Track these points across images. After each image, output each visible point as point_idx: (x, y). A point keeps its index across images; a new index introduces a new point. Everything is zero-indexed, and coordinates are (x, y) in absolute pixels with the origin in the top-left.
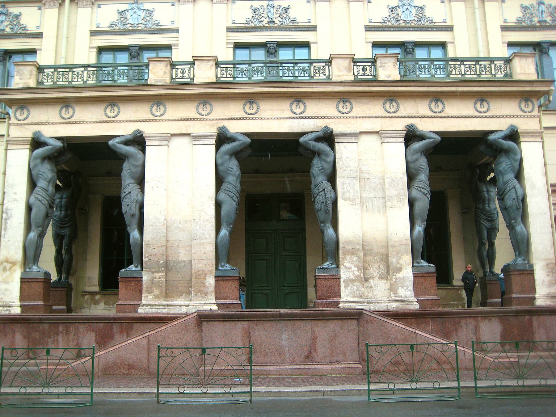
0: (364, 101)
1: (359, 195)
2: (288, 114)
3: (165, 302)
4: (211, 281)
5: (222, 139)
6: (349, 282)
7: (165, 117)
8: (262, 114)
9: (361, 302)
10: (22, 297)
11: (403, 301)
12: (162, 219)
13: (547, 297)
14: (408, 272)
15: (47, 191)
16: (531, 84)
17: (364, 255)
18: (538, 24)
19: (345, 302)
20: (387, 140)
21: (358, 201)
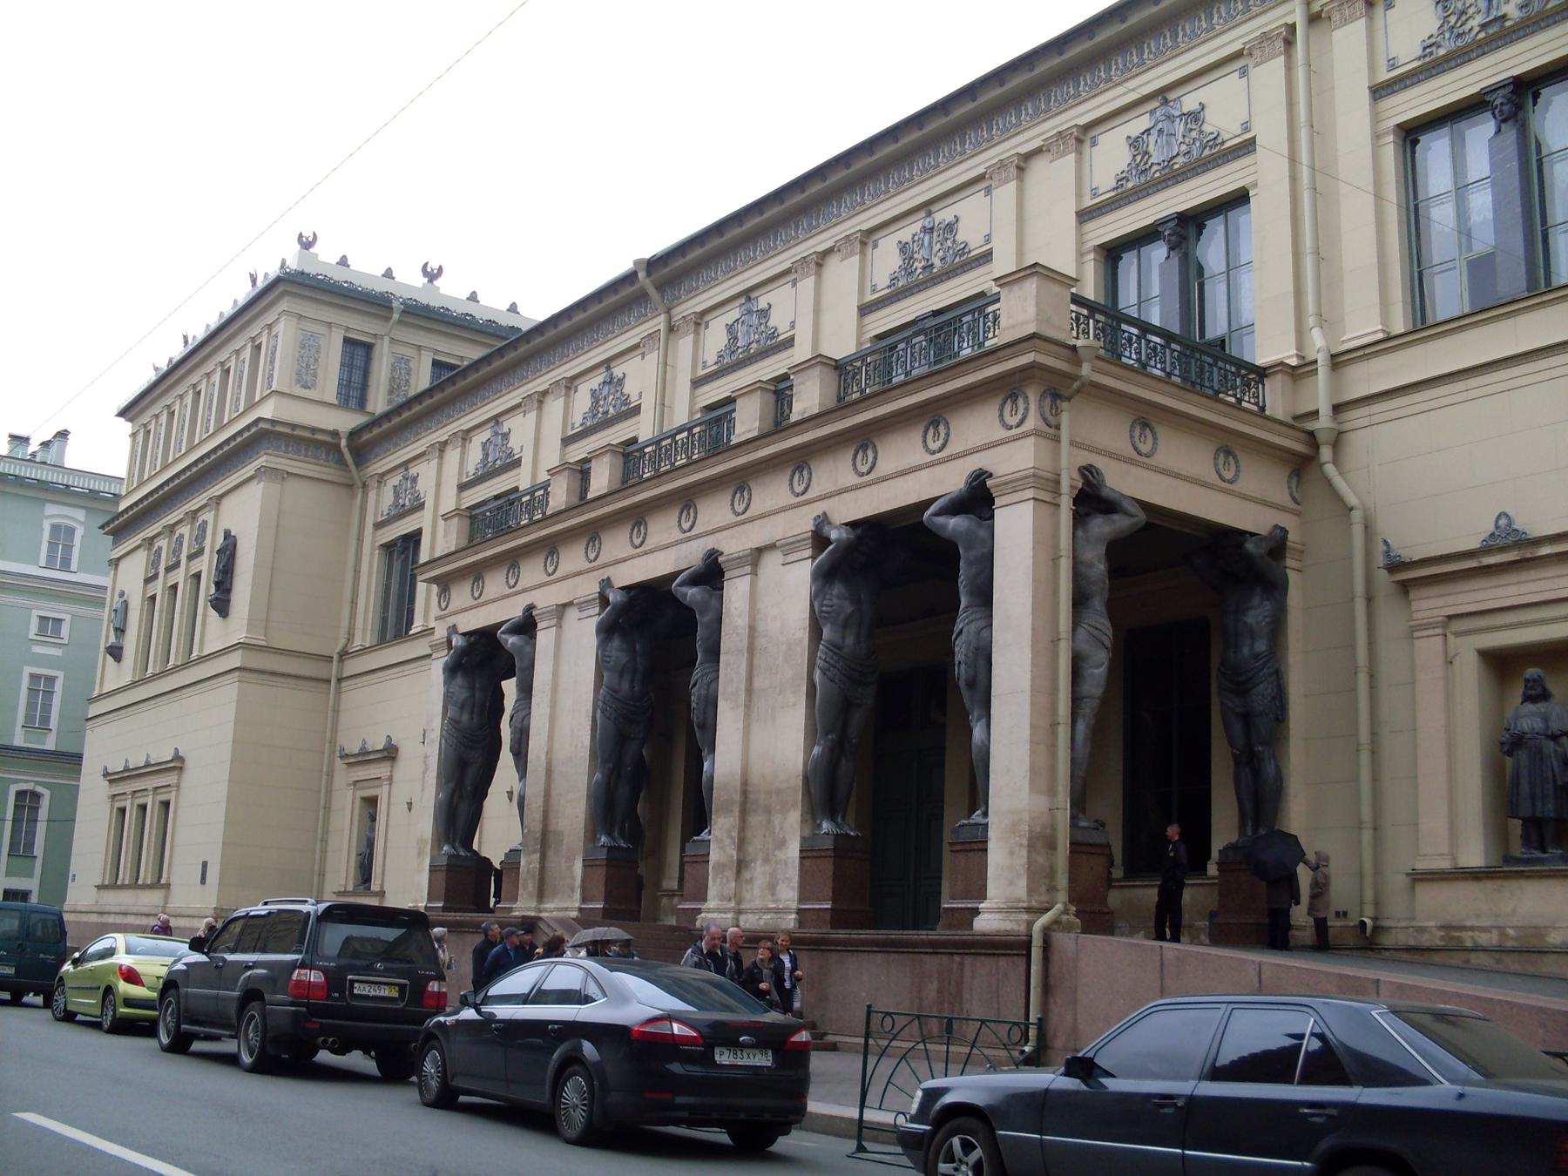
1: (743, 686)
5: (603, 600)
6: (721, 867)
8: (651, 543)
9: (725, 911)
11: (777, 911)
12: (543, 757)
13: (999, 910)
14: (793, 850)
15: (458, 722)
16: (994, 356)
17: (744, 813)
19: (709, 911)
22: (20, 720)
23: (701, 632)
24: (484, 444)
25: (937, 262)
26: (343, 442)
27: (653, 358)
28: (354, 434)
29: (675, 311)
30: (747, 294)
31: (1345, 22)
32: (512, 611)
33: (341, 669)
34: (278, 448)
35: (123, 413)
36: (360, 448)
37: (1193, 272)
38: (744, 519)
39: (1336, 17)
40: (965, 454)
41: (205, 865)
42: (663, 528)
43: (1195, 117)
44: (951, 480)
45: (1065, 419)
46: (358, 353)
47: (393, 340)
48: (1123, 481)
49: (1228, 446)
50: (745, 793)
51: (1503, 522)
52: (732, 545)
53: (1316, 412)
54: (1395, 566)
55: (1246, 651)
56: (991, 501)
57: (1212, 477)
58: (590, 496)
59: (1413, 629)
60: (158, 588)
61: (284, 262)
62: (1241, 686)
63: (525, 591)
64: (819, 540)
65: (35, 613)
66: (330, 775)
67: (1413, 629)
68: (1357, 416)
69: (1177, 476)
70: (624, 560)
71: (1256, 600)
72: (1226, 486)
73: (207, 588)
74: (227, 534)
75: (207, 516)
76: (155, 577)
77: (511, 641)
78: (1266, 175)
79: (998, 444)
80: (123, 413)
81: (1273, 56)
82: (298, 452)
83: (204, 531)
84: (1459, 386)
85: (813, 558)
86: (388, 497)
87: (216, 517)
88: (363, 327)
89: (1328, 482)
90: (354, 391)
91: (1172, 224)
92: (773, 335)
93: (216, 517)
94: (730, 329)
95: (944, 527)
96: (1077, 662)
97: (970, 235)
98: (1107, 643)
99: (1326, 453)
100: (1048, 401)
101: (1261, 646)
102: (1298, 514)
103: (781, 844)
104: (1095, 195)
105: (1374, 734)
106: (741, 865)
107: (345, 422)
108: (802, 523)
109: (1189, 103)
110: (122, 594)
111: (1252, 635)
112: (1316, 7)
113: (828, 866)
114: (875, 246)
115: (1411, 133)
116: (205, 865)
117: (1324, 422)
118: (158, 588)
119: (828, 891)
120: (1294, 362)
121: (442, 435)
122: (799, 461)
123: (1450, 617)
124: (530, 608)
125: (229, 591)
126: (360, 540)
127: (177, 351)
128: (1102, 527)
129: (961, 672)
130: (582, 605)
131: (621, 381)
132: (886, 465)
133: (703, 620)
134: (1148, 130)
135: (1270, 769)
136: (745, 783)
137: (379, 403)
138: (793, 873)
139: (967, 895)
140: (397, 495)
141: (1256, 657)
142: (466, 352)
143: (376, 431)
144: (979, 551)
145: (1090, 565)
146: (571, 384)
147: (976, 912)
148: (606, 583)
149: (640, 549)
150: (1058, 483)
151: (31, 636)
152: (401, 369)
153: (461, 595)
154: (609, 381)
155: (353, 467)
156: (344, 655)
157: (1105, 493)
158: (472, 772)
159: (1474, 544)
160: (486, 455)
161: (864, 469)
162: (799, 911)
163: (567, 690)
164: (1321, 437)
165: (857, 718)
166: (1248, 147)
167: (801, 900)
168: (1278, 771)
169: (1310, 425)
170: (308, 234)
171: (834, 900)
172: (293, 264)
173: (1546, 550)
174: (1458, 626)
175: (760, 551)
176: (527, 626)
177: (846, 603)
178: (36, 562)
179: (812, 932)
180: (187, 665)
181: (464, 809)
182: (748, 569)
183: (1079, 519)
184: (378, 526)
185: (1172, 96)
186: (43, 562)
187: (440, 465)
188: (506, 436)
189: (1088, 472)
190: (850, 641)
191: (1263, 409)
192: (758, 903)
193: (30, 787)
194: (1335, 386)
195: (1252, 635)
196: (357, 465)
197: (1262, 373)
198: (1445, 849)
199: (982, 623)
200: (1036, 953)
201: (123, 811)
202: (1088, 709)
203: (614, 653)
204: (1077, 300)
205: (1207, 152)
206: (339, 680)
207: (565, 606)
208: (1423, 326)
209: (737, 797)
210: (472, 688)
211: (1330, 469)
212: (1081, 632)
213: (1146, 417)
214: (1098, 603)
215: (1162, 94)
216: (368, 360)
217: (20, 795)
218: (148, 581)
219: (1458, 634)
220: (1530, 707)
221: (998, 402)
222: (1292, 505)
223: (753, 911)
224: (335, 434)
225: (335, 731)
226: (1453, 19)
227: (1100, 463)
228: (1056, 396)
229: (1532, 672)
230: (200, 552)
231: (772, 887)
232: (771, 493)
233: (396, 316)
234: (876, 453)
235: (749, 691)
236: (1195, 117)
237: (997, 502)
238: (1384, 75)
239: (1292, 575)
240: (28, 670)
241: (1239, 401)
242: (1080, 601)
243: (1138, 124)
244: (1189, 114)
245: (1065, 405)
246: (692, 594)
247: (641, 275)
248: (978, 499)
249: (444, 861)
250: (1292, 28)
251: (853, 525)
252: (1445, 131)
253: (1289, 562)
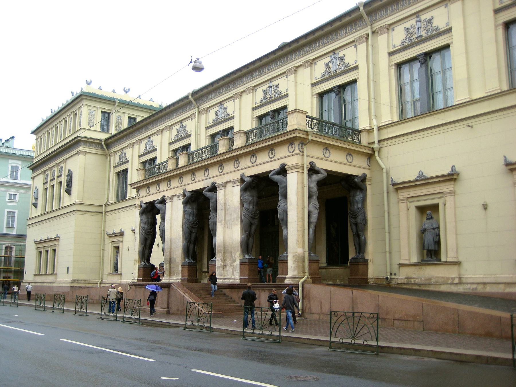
0: (228, 163)
2: (204, 178)
3: (168, 278)
4: (180, 268)
5: (184, 195)
7: (171, 187)
8: (196, 180)
10: (138, 277)
11: (234, 279)
14: (238, 263)
17: (225, 253)
18: (416, 40)
20: (234, 185)
21: (223, 222)
22: (5, 225)
23: (211, 204)
24: (146, 144)
25: (273, 97)
26: (103, 143)
27: (194, 121)
28: (106, 140)
29: (200, 107)
30: (220, 103)
31: (381, 34)
32: (159, 197)
33: (105, 209)
34: (84, 145)
35: (33, 133)
37: (342, 101)
38: (222, 174)
39: (379, 32)
40: (279, 159)
41: (68, 268)
42: (200, 175)
43: (342, 58)
44: (275, 166)
45: (305, 150)
46: (106, 116)
48: (320, 165)
49: (350, 153)
50: (225, 247)
51: (420, 173)
52: (219, 181)
53: (374, 142)
54: (394, 184)
55: (356, 207)
56: (286, 171)
57: (346, 162)
58: (179, 166)
59: (399, 201)
60: (48, 186)
61: (82, 89)
62: (355, 217)
63: (162, 192)
64: (242, 180)
66: (104, 240)
67: (399, 201)
68: (384, 143)
69: (336, 162)
70: (190, 184)
71: (358, 193)
72: (349, 164)
73: (64, 186)
74: (69, 171)
75: (63, 165)
76: (47, 182)
77: (159, 206)
78: (361, 75)
80: (33, 133)
81: (363, 43)
82: (89, 146)
83: (62, 169)
84: (411, 136)
85: (241, 185)
86: (117, 159)
87: (65, 165)
88: (107, 108)
89: (377, 161)
90: (106, 126)
91: (336, 88)
92: (228, 115)
93: (65, 165)
94: (216, 113)
95: (274, 179)
96: (310, 213)
97: (282, 89)
98: (317, 208)
99: (376, 154)
100: (300, 145)
101: (360, 205)
102: (370, 169)
103: (235, 261)
104: (316, 79)
105: (389, 228)
106: (224, 266)
107: (103, 136)
108: (237, 176)
109: (341, 54)
110: (36, 188)
111: (357, 203)
112: (374, 30)
113: (247, 267)
114: (256, 91)
115: (399, 66)
116: (68, 268)
117: (376, 145)
118: (48, 186)
119: (247, 273)
120: (368, 128)
121: (133, 141)
122: (236, 159)
123: (408, 198)
124: (164, 197)
125: (71, 187)
126: (109, 171)
127: (49, 114)
128: (315, 178)
129: (280, 216)
130: (178, 196)
131: (185, 127)
132: (259, 161)
133: (212, 201)
134: (330, 61)
135: (363, 238)
136: (225, 245)
137: (113, 131)
138: (238, 268)
139: (282, 274)
140: (120, 158)
141: (358, 208)
143: (113, 139)
144: (283, 185)
145: (313, 188)
146: (171, 127)
147: (285, 278)
148: (184, 191)
149: (194, 181)
150: (303, 167)
151: (7, 200)
153: (143, 192)
154: (182, 127)
155: (106, 150)
156: (106, 205)
157: (316, 169)
158: (148, 242)
159: (413, 178)
160: (146, 147)
161: (253, 162)
162: (240, 279)
163: (174, 221)
164: (375, 149)
165: (253, 227)
166: (356, 68)
167: (240, 276)
168: (365, 238)
169: (372, 146)
170: (89, 80)
171: (249, 276)
172: (85, 90)
173: (432, 181)
174: (410, 200)
175: (226, 182)
176: (163, 201)
177: (250, 197)
179: (244, 284)
180: (59, 209)
181: (147, 252)
182: (223, 188)
183: (309, 176)
184: (115, 167)
185: (336, 52)
187: (133, 149)
188: (152, 142)
189: (311, 163)
190: (251, 207)
191: (360, 141)
192: (229, 277)
194: (379, 135)
195: (357, 203)
196: (108, 149)
197: (360, 132)
198: (407, 258)
199: (285, 204)
200: (300, 289)
201: (41, 252)
202: (312, 226)
203: (188, 210)
204: (308, 117)
205: (346, 68)
206: (105, 212)
207: (173, 196)
208: (403, 119)
209: (223, 249)
210: (148, 218)
211: (378, 158)
212: (311, 205)
213: (327, 147)
214: (315, 198)
215: (334, 51)
216: (109, 118)
217: (6, 248)
218: (44, 184)
219: (410, 202)
220: (428, 221)
221: (287, 145)
222: (368, 167)
223: (228, 279)
224: (100, 140)
225: (105, 227)
226: (409, 35)
227: (315, 161)
228: (302, 144)
229: (428, 212)
230: (61, 175)
231: (233, 273)
232: (229, 167)
233: (117, 104)
234: (256, 157)
235: (225, 220)
236: (342, 58)
237: (288, 172)
238: (392, 50)
239: (368, 187)
240: (6, 210)
241: (353, 140)
242: (310, 197)
243: (327, 60)
244: (341, 57)
245: (305, 146)
246: (209, 194)
247: (190, 97)
248: (283, 171)
249: (142, 266)
250: (368, 35)
251: (251, 176)
252: (408, 64)
253: (367, 183)
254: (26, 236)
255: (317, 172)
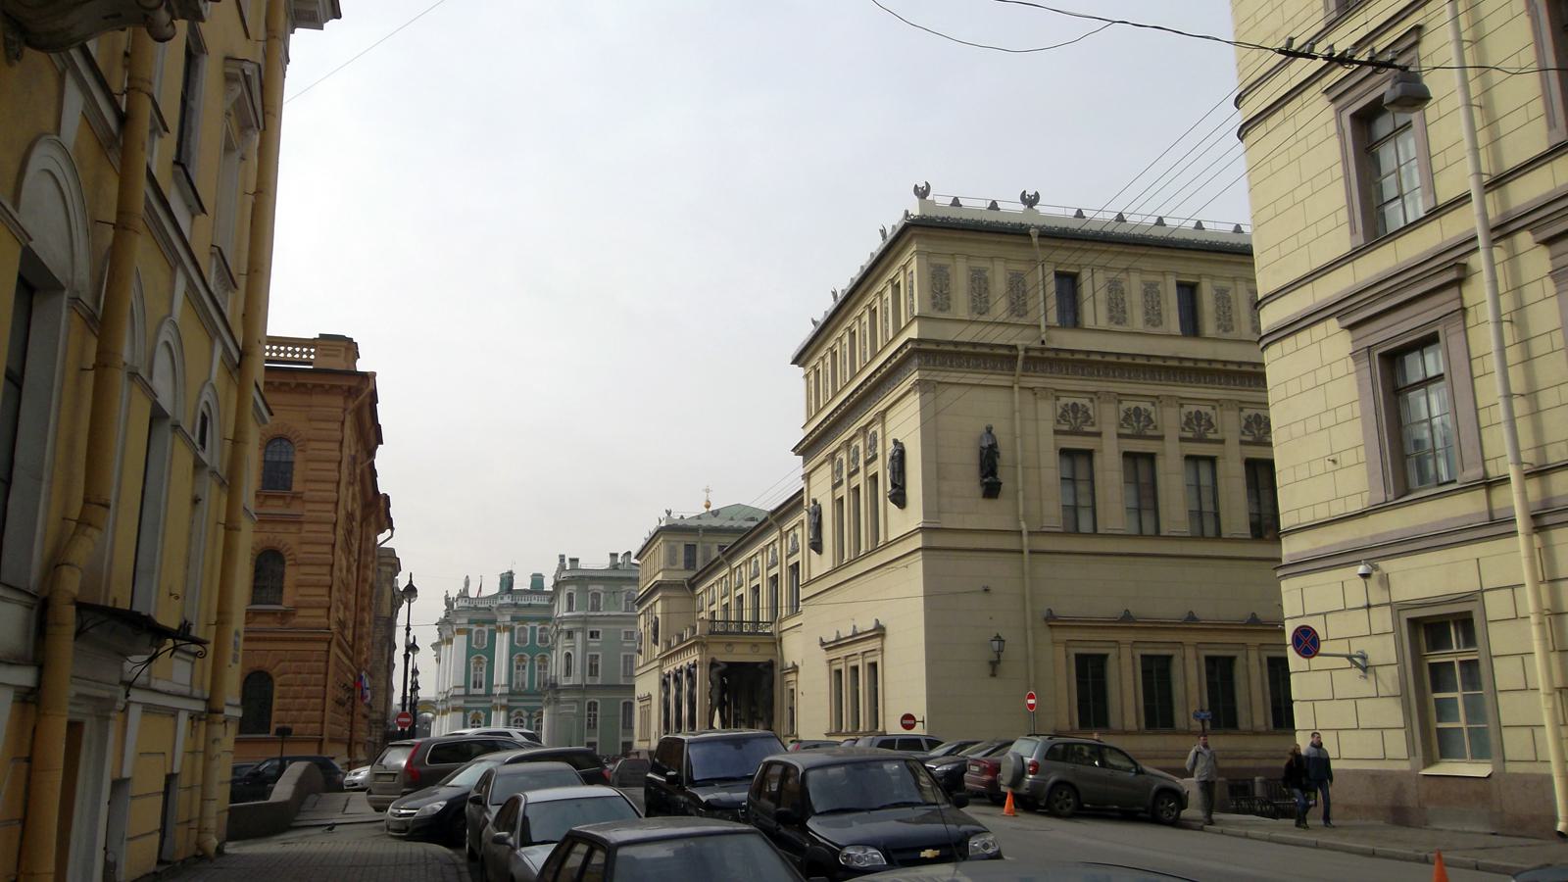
22: (622, 674)
28: (689, 581)
36: (692, 584)
46: (690, 549)
47: (702, 542)
65: (623, 631)
68: (784, 634)
79: (693, 656)
88: (690, 539)
90: (690, 563)
128: (715, 670)
137: (700, 566)
142: (728, 541)
152: (707, 551)
178: (620, 609)
186: (623, 609)
189: (713, 659)
193: (627, 700)
217: (624, 703)
227: (716, 657)
240: (622, 654)
254: (634, 686)
255: (718, 665)
